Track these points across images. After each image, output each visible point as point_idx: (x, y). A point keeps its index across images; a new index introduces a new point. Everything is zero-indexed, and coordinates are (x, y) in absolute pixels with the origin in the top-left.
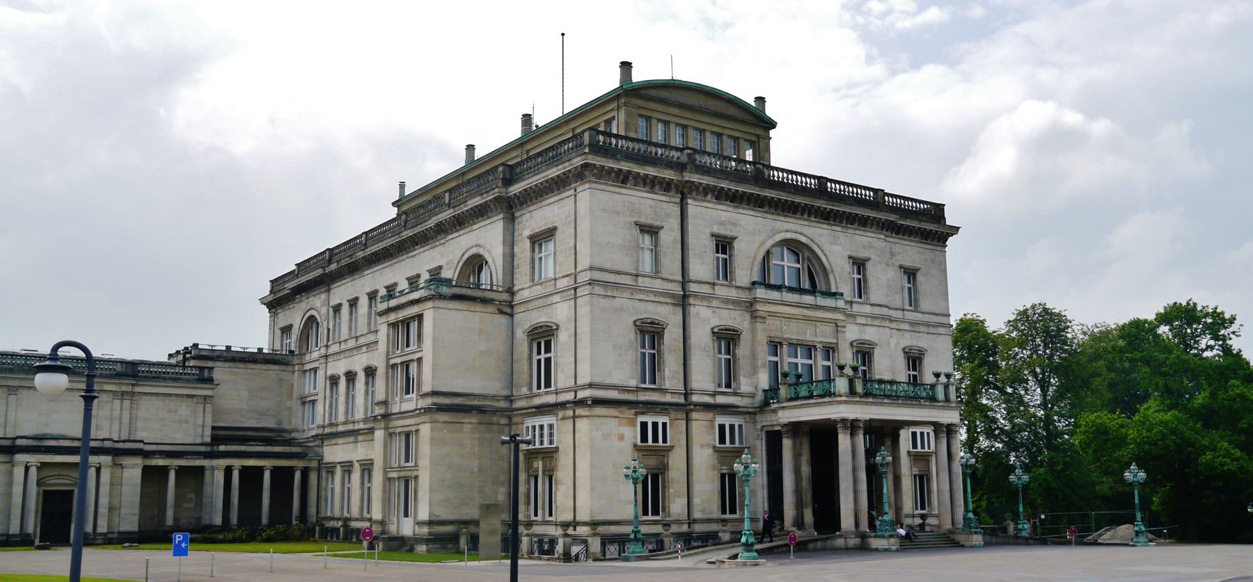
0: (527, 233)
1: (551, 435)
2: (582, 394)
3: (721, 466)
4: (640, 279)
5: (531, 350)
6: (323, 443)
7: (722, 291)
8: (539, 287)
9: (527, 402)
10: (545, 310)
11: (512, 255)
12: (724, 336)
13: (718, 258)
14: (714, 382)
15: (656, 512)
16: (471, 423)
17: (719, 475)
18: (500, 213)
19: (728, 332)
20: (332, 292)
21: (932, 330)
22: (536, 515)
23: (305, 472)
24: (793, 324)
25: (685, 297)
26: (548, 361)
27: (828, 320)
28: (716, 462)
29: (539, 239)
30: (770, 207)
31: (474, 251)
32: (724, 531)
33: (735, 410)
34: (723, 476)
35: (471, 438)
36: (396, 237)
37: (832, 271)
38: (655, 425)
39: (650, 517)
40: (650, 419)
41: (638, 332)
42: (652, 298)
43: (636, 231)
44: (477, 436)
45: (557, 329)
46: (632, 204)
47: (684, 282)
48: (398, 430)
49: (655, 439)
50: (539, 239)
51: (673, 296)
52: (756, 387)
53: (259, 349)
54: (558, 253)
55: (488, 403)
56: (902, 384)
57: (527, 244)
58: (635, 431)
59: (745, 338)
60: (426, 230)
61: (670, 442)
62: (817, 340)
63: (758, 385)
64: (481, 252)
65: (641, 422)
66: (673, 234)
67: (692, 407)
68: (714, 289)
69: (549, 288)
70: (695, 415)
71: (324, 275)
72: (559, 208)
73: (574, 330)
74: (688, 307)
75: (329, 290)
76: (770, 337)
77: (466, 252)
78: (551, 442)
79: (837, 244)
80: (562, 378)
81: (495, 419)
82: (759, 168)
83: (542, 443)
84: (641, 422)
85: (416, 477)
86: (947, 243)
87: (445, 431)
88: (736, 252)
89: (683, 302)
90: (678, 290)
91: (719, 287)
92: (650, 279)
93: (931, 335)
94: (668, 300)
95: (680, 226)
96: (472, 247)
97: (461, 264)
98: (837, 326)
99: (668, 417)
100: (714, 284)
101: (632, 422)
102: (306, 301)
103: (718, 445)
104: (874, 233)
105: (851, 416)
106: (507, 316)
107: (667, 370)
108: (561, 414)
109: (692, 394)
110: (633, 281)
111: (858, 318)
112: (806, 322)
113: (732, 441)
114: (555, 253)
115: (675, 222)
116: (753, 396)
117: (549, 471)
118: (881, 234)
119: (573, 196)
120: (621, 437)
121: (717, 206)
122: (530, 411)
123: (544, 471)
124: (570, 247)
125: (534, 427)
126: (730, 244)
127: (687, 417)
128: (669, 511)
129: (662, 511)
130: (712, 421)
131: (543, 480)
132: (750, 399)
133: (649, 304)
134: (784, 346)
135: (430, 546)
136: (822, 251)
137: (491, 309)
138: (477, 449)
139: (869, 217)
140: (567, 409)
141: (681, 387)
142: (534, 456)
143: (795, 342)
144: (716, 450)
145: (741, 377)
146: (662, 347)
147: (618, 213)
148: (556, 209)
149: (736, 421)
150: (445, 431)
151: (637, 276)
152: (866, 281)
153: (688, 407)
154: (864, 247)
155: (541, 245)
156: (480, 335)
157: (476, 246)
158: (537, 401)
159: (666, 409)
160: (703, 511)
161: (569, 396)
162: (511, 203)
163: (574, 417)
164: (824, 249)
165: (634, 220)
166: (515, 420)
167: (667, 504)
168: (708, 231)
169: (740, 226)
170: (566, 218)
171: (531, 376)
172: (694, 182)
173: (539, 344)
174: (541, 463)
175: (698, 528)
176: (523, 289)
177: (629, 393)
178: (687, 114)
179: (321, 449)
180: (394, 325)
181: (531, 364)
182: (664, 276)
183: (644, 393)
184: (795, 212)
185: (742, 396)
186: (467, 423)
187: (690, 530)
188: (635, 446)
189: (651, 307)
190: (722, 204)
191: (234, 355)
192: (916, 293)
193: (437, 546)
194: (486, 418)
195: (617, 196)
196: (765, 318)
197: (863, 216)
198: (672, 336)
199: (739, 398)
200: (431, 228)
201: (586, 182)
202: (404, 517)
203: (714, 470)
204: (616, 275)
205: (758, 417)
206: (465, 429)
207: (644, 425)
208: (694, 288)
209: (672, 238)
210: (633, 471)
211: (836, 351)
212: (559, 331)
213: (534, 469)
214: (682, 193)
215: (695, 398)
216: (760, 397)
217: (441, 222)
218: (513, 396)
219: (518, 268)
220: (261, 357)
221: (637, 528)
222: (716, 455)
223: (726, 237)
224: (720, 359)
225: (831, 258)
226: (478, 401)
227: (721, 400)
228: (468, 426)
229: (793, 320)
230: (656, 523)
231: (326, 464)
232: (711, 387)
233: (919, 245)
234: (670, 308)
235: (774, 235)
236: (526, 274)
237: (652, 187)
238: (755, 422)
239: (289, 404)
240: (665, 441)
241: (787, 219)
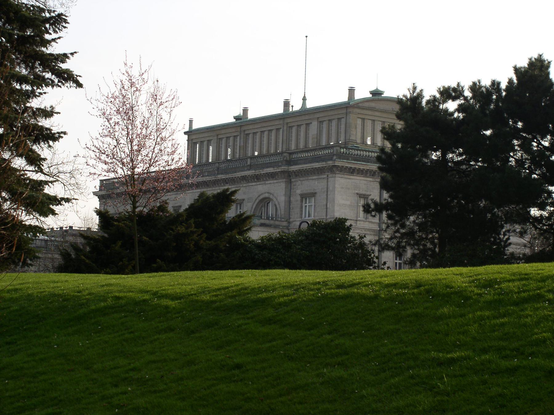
0: (299, 192)
11: (290, 202)
18: (283, 178)
29: (304, 197)
43: (357, 198)
50: (304, 197)
51: (374, 231)
57: (299, 198)
60: (235, 177)
72: (318, 183)
94: (372, 233)
96: (265, 193)
97: (257, 201)
114: (315, 206)
147: (349, 189)
148: (316, 183)
165: (356, 192)
178: (385, 115)
195: (348, 180)
200: (238, 177)
217: (246, 176)
219: (293, 209)
224: (396, 263)
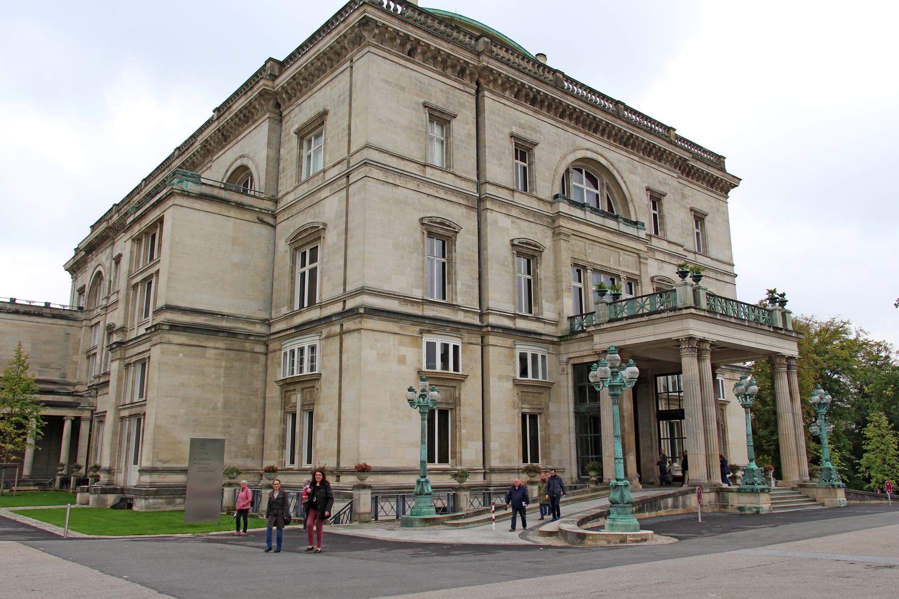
1: (313, 360)
2: (350, 304)
3: (522, 404)
4: (429, 170)
5: (294, 262)
6: (97, 393)
7: (521, 199)
8: (305, 186)
9: (287, 323)
10: (312, 211)
11: (278, 160)
12: (524, 251)
13: (517, 165)
14: (514, 304)
15: (444, 459)
16: (215, 348)
17: (521, 415)
19: (529, 247)
20: (116, 245)
21: (719, 277)
22: (292, 462)
23: (76, 422)
24: (597, 248)
25: (480, 200)
26: (313, 272)
27: (630, 249)
28: (516, 399)
30: (570, 119)
31: (238, 163)
32: (532, 483)
33: (539, 337)
34: (524, 416)
35: (216, 367)
36: (166, 171)
37: (632, 200)
38: (445, 347)
39: (436, 465)
40: (439, 340)
41: (426, 232)
42: (442, 195)
43: (425, 115)
44: (223, 364)
45: (324, 229)
46: (420, 82)
47: (481, 182)
48: (134, 359)
49: (445, 365)
51: (466, 196)
52: (559, 314)
53: (46, 303)
54: (328, 141)
55: (240, 325)
56: (743, 305)
57: (295, 140)
58: (420, 354)
59: (547, 257)
61: (462, 370)
62: (621, 269)
63: (562, 311)
64: (245, 161)
65: (427, 343)
66: (467, 127)
67: (489, 329)
68: (513, 196)
69: (317, 182)
70: (492, 340)
71: (108, 228)
73: (344, 226)
74: (483, 213)
75: (113, 243)
76: (574, 258)
77: (230, 167)
78: (312, 368)
79: (635, 174)
80: (327, 289)
81: (248, 345)
82: (559, 76)
83: (301, 370)
84: (427, 343)
85: (144, 414)
86: (729, 194)
87: (181, 355)
88: (536, 160)
89: (479, 205)
90: (471, 189)
91: (519, 194)
92: (440, 172)
93: (719, 282)
95: (475, 120)
96: (236, 160)
98: (639, 257)
99: (460, 340)
100: (513, 191)
101: (415, 341)
102: (96, 258)
103: (518, 377)
104: (668, 170)
105: (699, 335)
106: (269, 228)
107: (459, 282)
108: (325, 332)
109: (488, 314)
110: (420, 171)
111: (657, 253)
112: (610, 248)
113: (535, 374)
115: (471, 115)
116: (556, 324)
117: (308, 405)
118: (674, 172)
119: (349, 69)
120: (402, 360)
121: (516, 106)
122: (289, 332)
123: (303, 405)
124: (344, 129)
125: (293, 352)
126: (530, 150)
127: (482, 342)
128: (461, 458)
129: (452, 458)
130: (512, 348)
131: (302, 417)
132: (553, 327)
133: (438, 201)
134: (589, 271)
135: (151, 501)
136: (622, 178)
137: (248, 216)
138: (222, 380)
139: (665, 150)
140: (333, 325)
141: (475, 305)
142: (292, 388)
143: (599, 268)
144: (516, 383)
145: (544, 301)
146: (454, 254)
147: (403, 89)
149: (540, 351)
150: (181, 355)
151: (425, 166)
152: (662, 217)
153: (485, 330)
154: (660, 182)
155: (310, 141)
156: (233, 245)
157: (241, 157)
158: (298, 320)
159: (458, 330)
160: (502, 458)
161: (337, 308)
162: (279, 100)
163: (342, 333)
164: (624, 176)
166: (272, 346)
167: (458, 449)
168: (507, 131)
169: (540, 133)
170: (339, 97)
171: (292, 292)
172: (493, 69)
173: (304, 254)
174: (299, 396)
175: (496, 479)
176: (288, 193)
177: (412, 305)
179: (94, 399)
180: (137, 240)
181: (293, 278)
182: (457, 173)
183: (432, 307)
184: (595, 131)
185: (545, 323)
186: (211, 348)
187: (485, 482)
188: (420, 372)
189: (440, 205)
190: (521, 105)
191: (18, 308)
192: (705, 238)
193: (160, 500)
194: (237, 344)
196: (569, 236)
197: (660, 148)
198: (465, 243)
199: (542, 325)
200: (197, 151)
201: (365, 46)
202: (134, 464)
203: (514, 407)
204: (400, 160)
205: (562, 348)
206: (208, 355)
207: (431, 347)
208: (491, 191)
209: (466, 131)
210: (421, 396)
211: (639, 284)
212: (327, 231)
213: (291, 405)
214: (478, 84)
215: (492, 320)
216: (565, 325)
218: (272, 319)
219: (283, 172)
220: (48, 311)
221: (424, 477)
222: (516, 390)
223: (525, 141)
225: (630, 187)
226: (227, 322)
227: (521, 324)
228: (213, 351)
229: (596, 244)
230: (444, 472)
231: (97, 414)
232: (510, 308)
233: (705, 191)
234: (463, 211)
235: (575, 150)
236: (291, 176)
237: (445, 68)
238: (559, 354)
239: (75, 358)
240: (456, 368)
241: (587, 137)
